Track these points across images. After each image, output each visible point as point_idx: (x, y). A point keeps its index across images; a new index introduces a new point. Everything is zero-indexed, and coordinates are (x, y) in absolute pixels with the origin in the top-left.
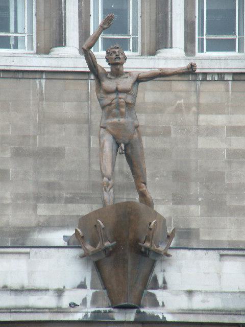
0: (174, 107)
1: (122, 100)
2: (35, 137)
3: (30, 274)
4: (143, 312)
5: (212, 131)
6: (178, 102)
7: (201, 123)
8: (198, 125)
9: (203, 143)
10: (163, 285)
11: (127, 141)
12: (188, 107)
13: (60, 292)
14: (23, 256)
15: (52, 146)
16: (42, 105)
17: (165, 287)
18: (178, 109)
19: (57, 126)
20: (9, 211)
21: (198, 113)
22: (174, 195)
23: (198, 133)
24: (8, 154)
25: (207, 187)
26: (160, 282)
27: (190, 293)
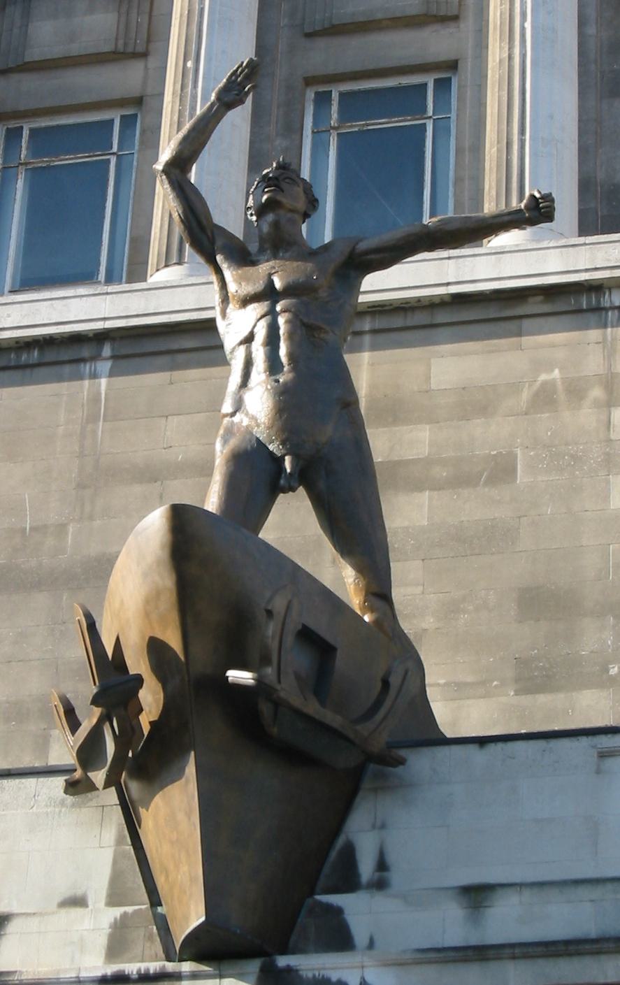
0: (526, 395)
2: (61, 529)
4: (289, 969)
6: (543, 377)
8: (609, 441)
10: (377, 874)
12: (576, 391)
16: (94, 432)
17: (380, 884)
18: (545, 399)
19: (138, 489)
26: (366, 868)
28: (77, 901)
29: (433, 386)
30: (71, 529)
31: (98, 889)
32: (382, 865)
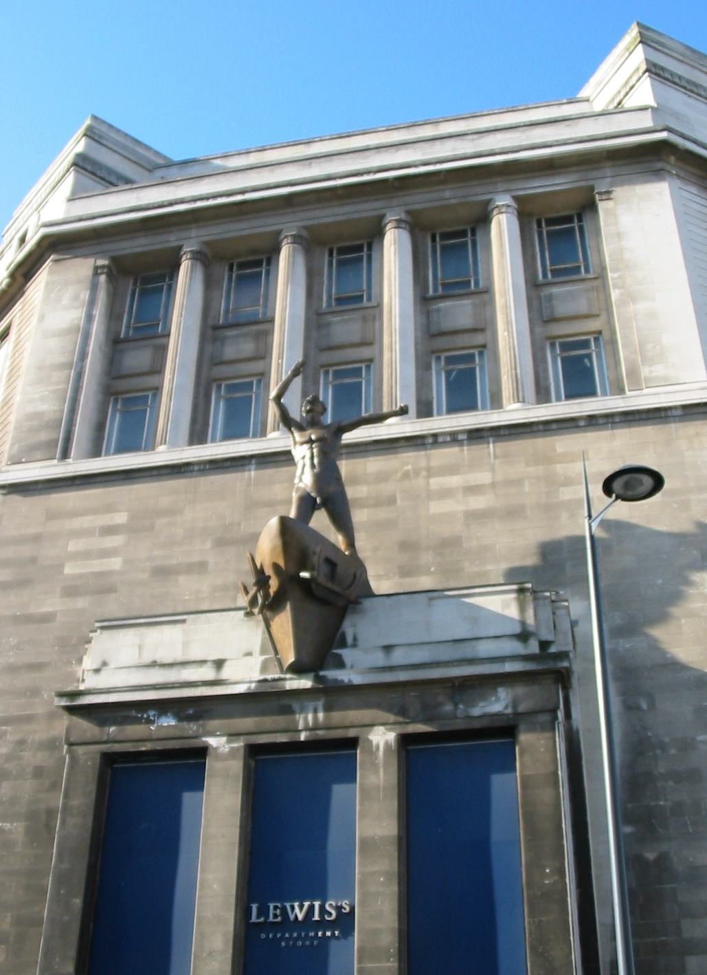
0: (399, 474)
2: (239, 524)
3: (186, 644)
5: (446, 493)
6: (406, 468)
9: (435, 507)
12: (417, 473)
13: (219, 664)
17: (354, 645)
18: (406, 475)
21: (429, 477)
24: (208, 545)
26: (349, 640)
27: (388, 648)
28: (249, 654)
29: (368, 472)
30: (242, 524)
31: (256, 647)
32: (355, 639)
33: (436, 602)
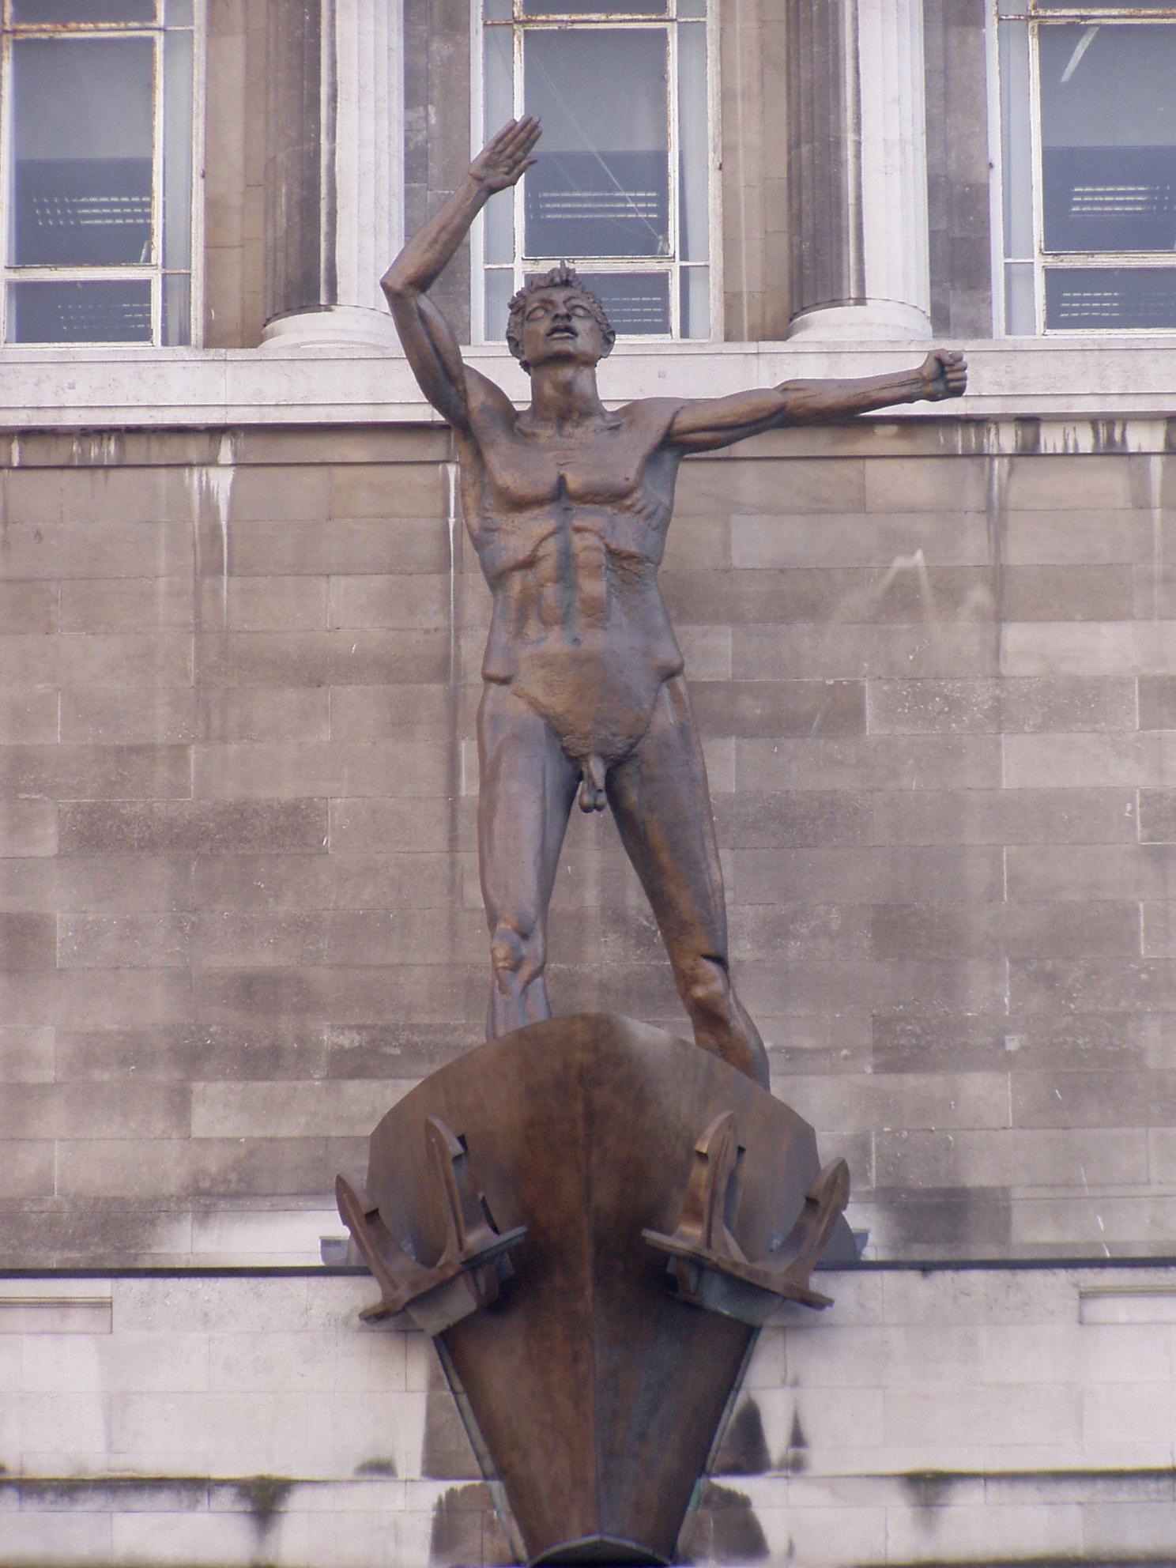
1: (590, 540)
2: (178, 753)
6: (900, 562)
7: (1017, 667)
8: (999, 677)
10: (792, 1451)
11: (619, 746)
14: (78, 1319)
15: (264, 793)
16: (216, 592)
17: (796, 1465)
19: (291, 696)
20: (53, 1120)
21: (999, 616)
22: (883, 1024)
23: (999, 715)
24: (47, 841)
25: (1050, 979)
26: (776, 1442)
28: (380, 1469)
29: (736, 562)
30: (192, 754)
31: (409, 1452)
32: (797, 1439)
33: (1099, 1309)
